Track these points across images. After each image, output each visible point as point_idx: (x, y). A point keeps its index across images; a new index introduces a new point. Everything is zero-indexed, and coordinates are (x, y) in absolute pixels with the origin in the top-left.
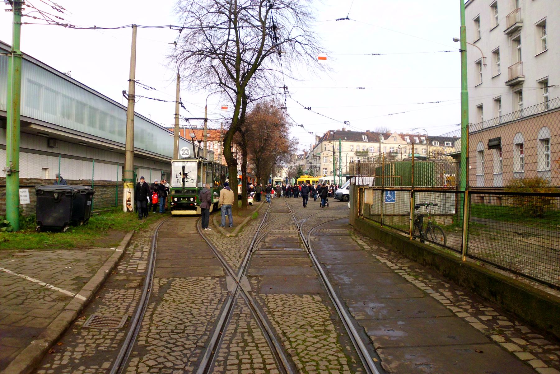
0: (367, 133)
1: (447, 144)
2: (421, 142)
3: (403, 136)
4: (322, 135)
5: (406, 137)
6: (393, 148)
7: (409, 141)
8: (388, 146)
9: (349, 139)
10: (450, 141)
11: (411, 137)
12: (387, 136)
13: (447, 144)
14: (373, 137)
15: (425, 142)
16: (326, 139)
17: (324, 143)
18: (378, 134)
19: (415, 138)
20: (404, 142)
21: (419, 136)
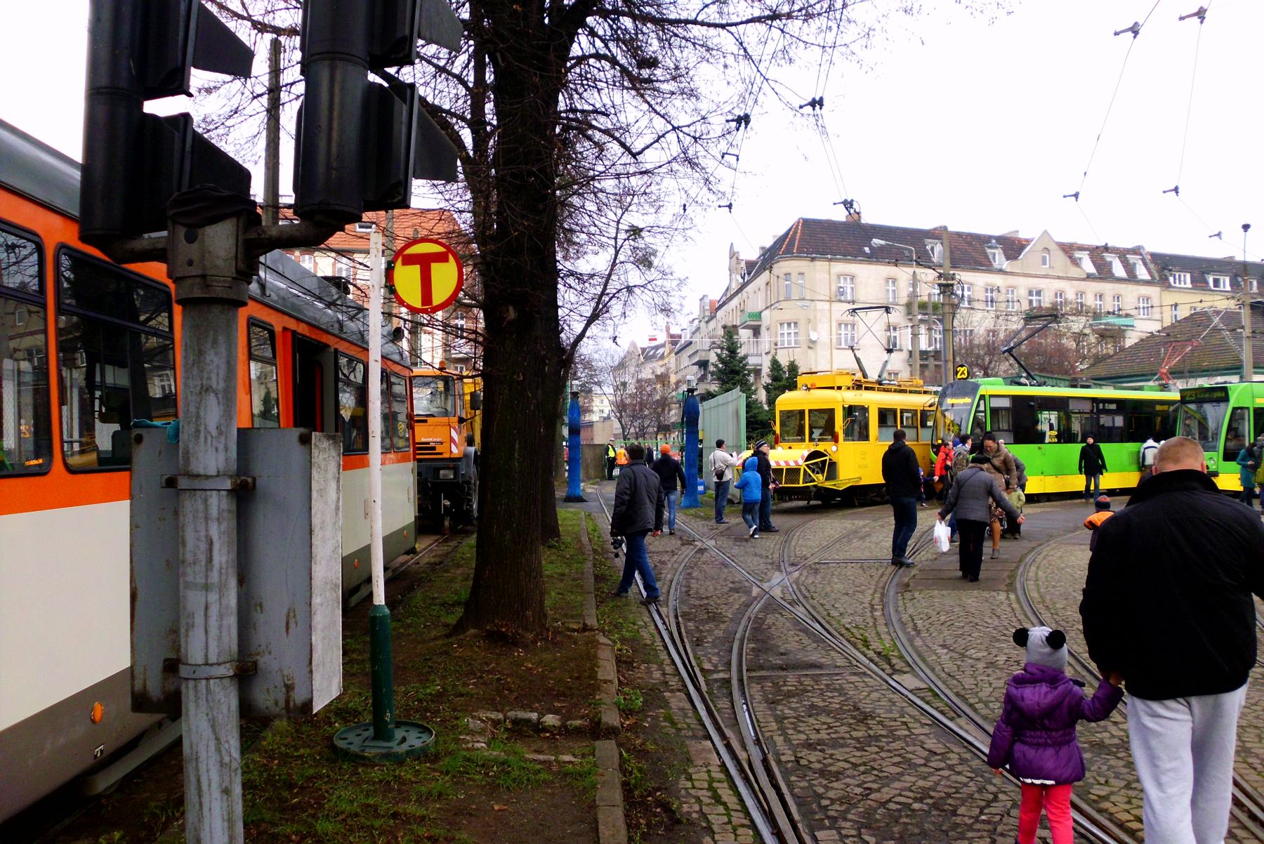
0: (937, 234)
1: (1216, 282)
2: (1132, 278)
3: (1069, 250)
4: (753, 254)
5: (1077, 255)
6: (1039, 293)
7: (1088, 266)
8: (1023, 285)
9: (877, 256)
10: (1221, 272)
11: (1097, 253)
12: (1013, 247)
13: (1216, 282)
14: (970, 251)
15: (1142, 273)
16: (789, 251)
17: (782, 267)
18: (984, 240)
19: (1109, 257)
20: (1074, 271)
21: (1122, 254)
